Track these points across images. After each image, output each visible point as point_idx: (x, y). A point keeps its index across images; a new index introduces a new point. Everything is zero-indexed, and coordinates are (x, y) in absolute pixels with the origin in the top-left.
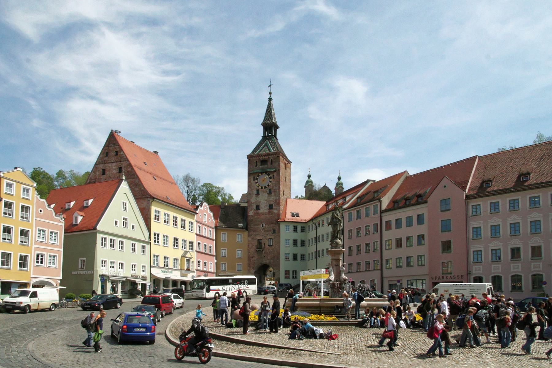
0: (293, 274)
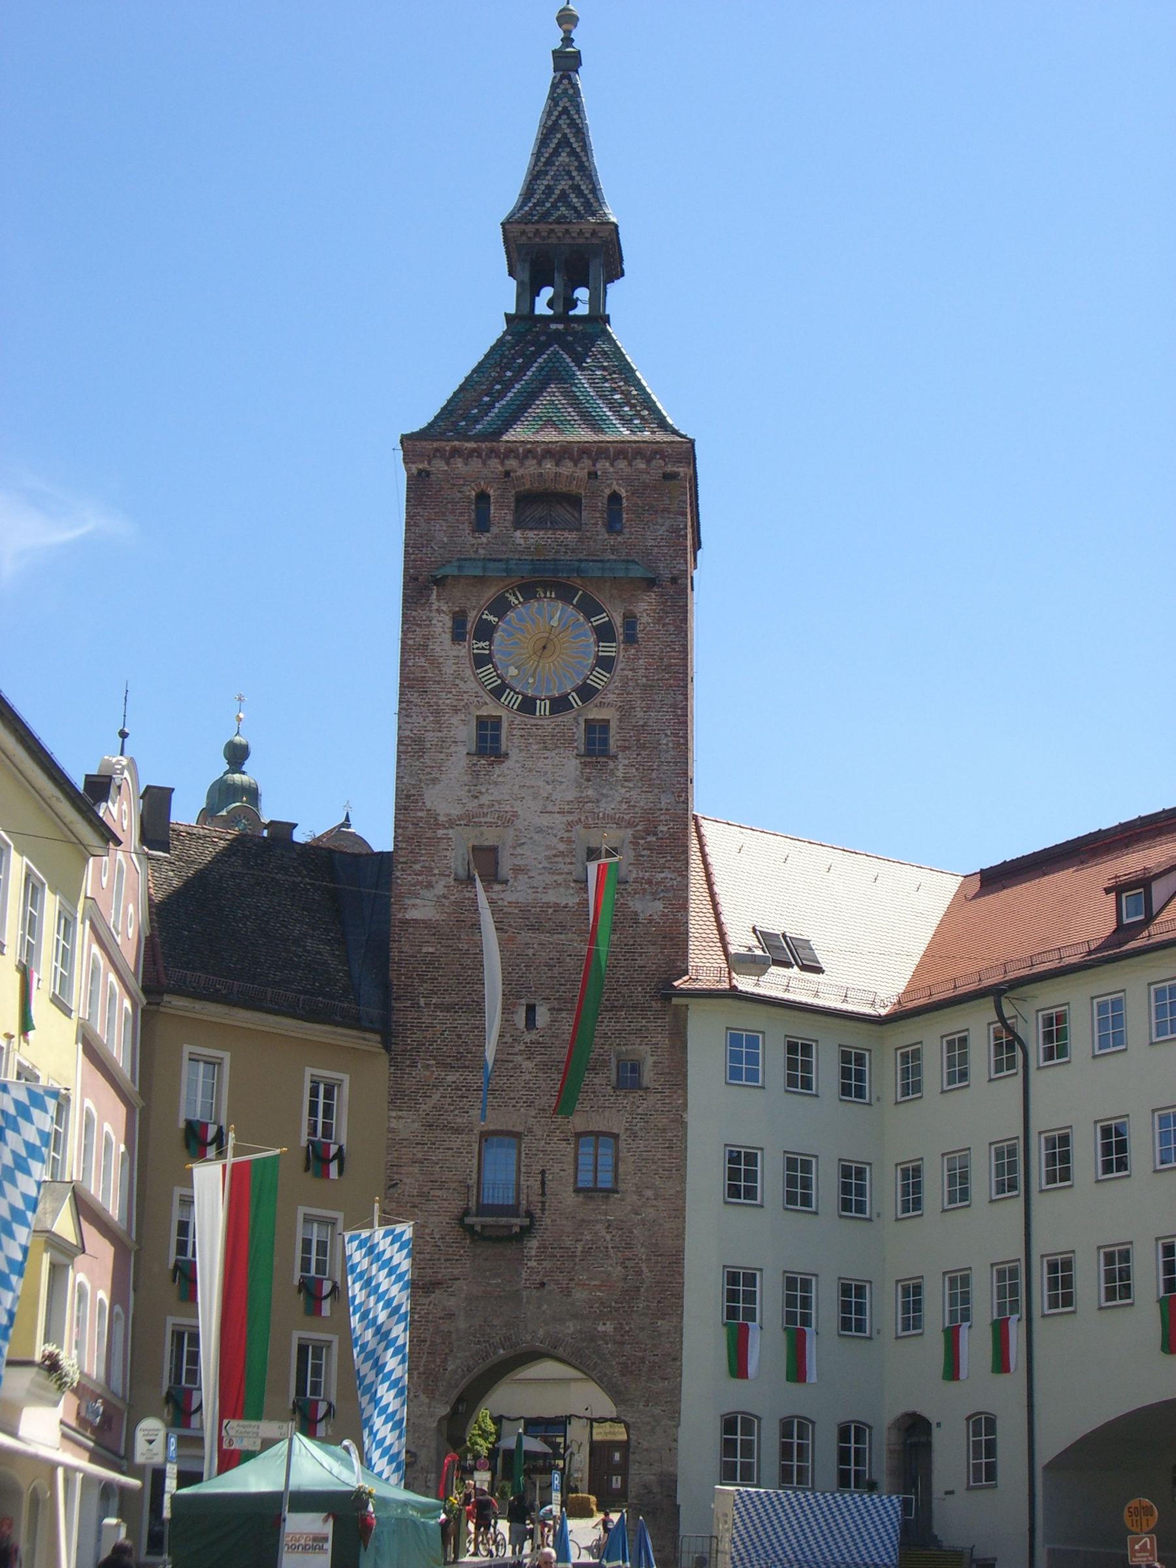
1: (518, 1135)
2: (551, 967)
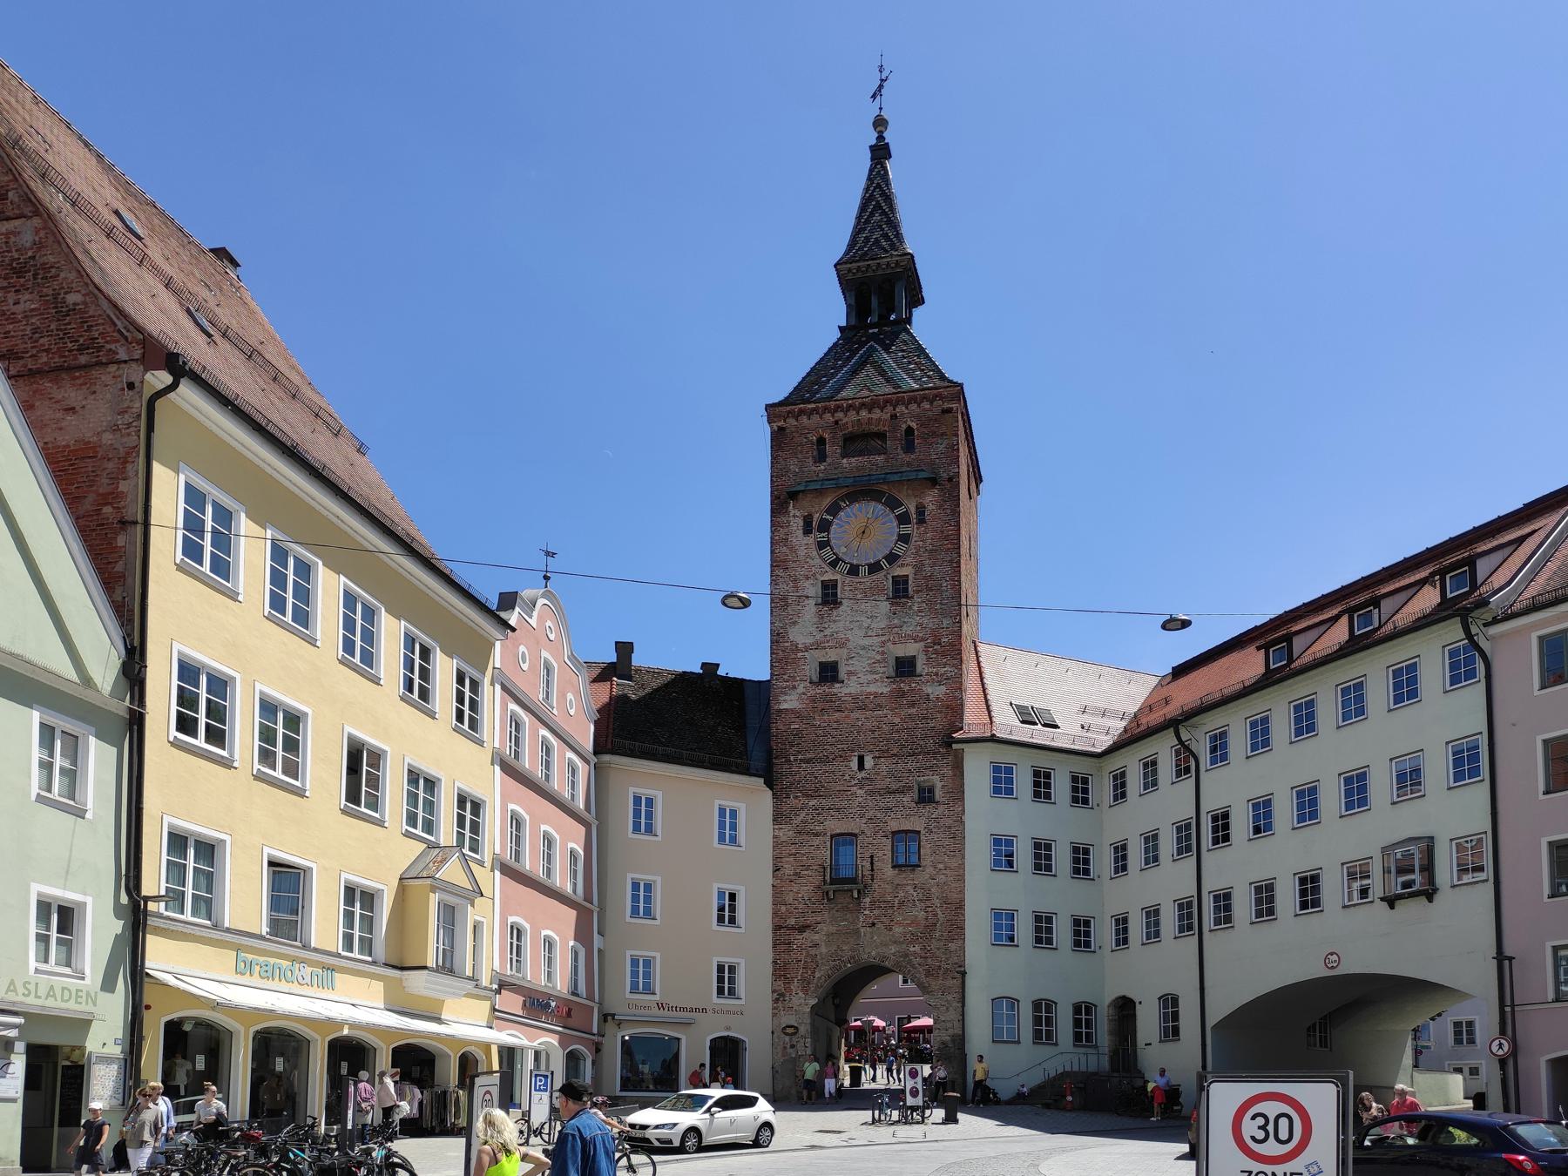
0: (1037, 1021)
1: (855, 835)
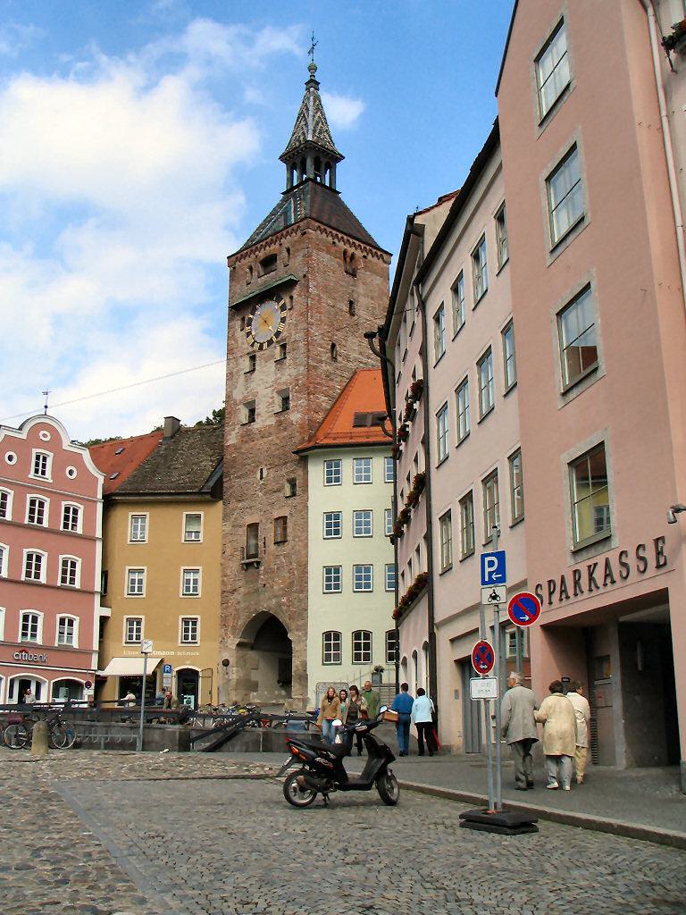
2: (267, 451)
